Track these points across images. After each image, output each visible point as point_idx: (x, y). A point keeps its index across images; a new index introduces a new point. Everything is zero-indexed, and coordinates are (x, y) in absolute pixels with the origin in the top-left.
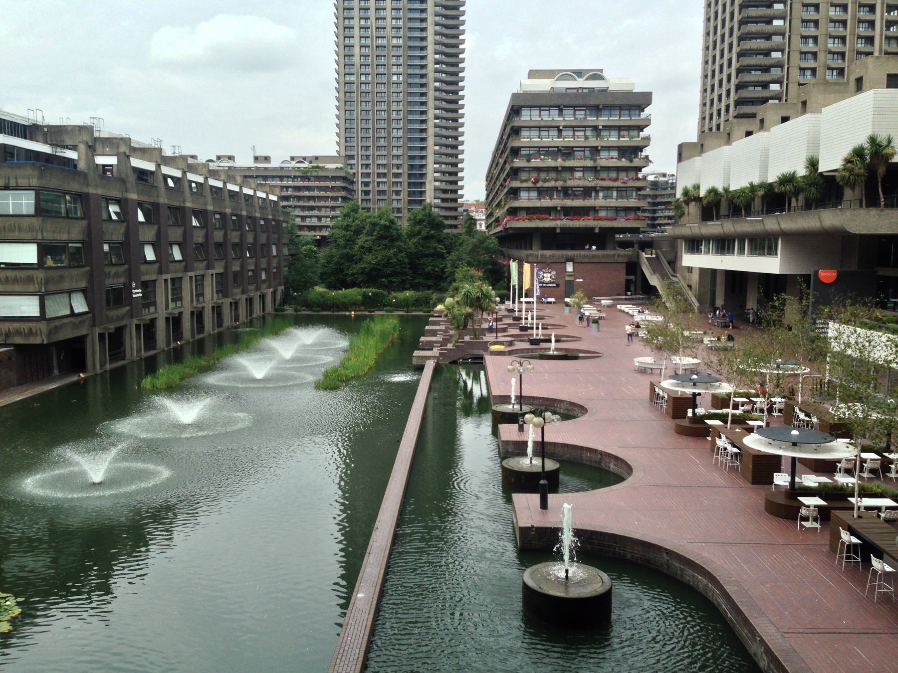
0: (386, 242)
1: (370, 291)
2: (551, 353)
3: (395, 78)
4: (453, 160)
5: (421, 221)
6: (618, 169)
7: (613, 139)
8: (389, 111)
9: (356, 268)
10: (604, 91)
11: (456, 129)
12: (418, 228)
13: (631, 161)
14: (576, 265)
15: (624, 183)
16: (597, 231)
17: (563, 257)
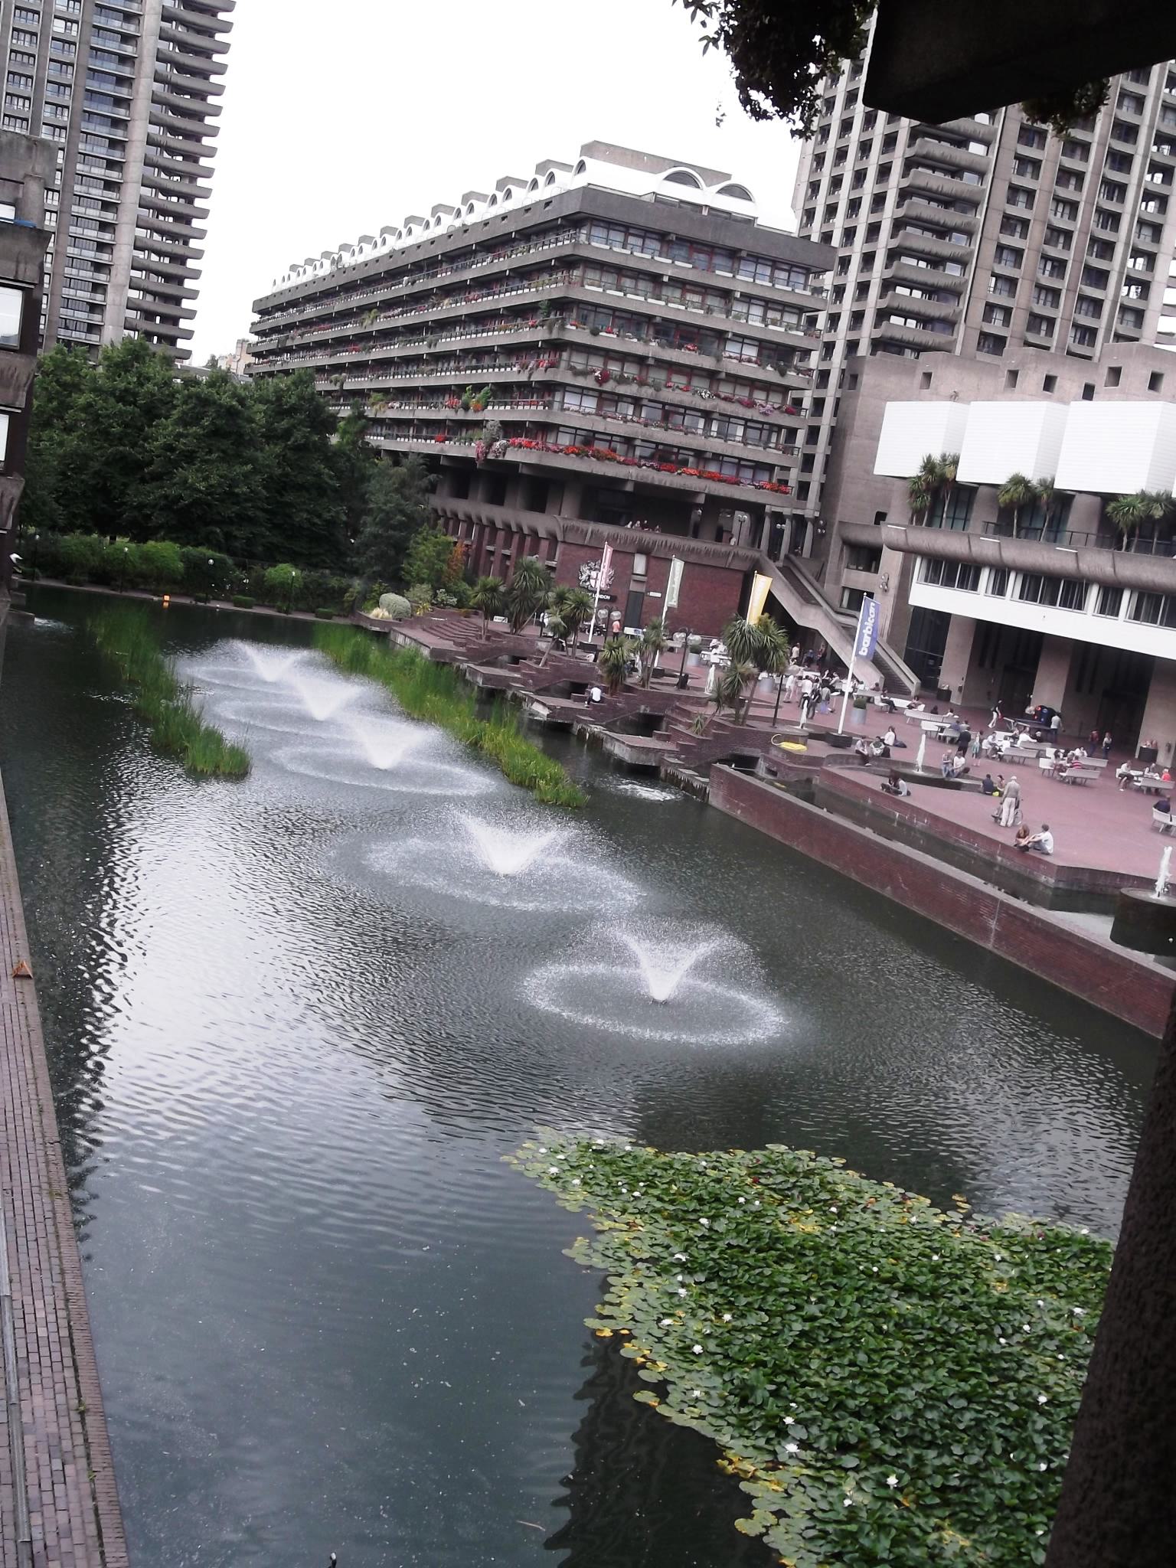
0: (226, 444)
1: (211, 556)
2: (915, 772)
3: (59, 26)
4: (177, 248)
5: (292, 411)
6: (753, 384)
7: (754, 321)
8: (36, 102)
9: (153, 493)
10: (750, 221)
11: (193, 178)
12: (284, 424)
13: (783, 374)
14: (653, 562)
15: (765, 414)
16: (701, 500)
17: (633, 541)
